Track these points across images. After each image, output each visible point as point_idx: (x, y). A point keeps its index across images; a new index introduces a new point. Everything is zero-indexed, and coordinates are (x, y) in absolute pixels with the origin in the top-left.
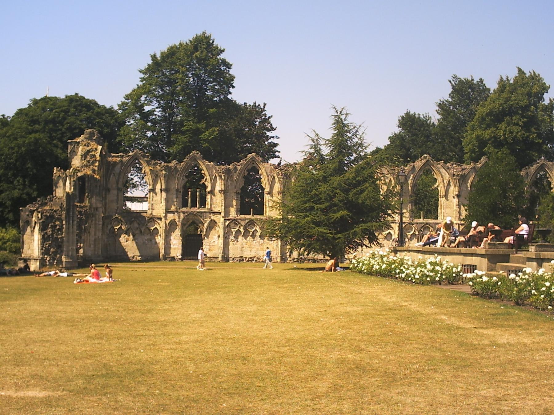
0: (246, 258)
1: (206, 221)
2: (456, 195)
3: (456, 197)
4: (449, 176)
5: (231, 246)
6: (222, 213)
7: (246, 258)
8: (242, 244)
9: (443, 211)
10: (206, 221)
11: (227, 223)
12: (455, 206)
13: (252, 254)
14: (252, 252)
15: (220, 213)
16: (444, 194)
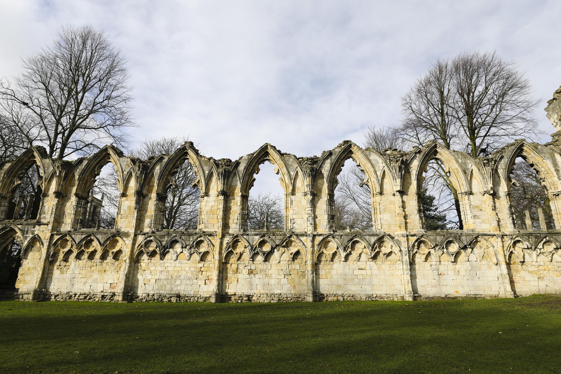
0: (75, 295)
1: (26, 237)
2: (397, 191)
3: (398, 193)
4: (384, 164)
5: (56, 273)
6: (49, 226)
7: (75, 295)
8: (74, 273)
9: (379, 216)
10: (26, 238)
11: (56, 238)
12: (397, 208)
13: (86, 290)
14: (87, 284)
15: (47, 225)
16: (378, 190)
